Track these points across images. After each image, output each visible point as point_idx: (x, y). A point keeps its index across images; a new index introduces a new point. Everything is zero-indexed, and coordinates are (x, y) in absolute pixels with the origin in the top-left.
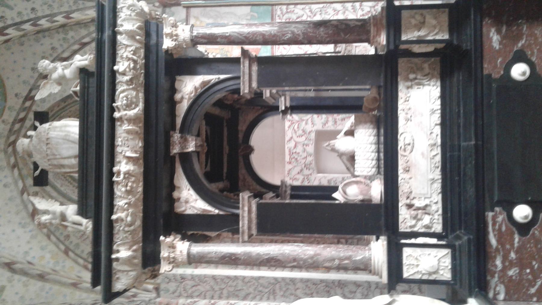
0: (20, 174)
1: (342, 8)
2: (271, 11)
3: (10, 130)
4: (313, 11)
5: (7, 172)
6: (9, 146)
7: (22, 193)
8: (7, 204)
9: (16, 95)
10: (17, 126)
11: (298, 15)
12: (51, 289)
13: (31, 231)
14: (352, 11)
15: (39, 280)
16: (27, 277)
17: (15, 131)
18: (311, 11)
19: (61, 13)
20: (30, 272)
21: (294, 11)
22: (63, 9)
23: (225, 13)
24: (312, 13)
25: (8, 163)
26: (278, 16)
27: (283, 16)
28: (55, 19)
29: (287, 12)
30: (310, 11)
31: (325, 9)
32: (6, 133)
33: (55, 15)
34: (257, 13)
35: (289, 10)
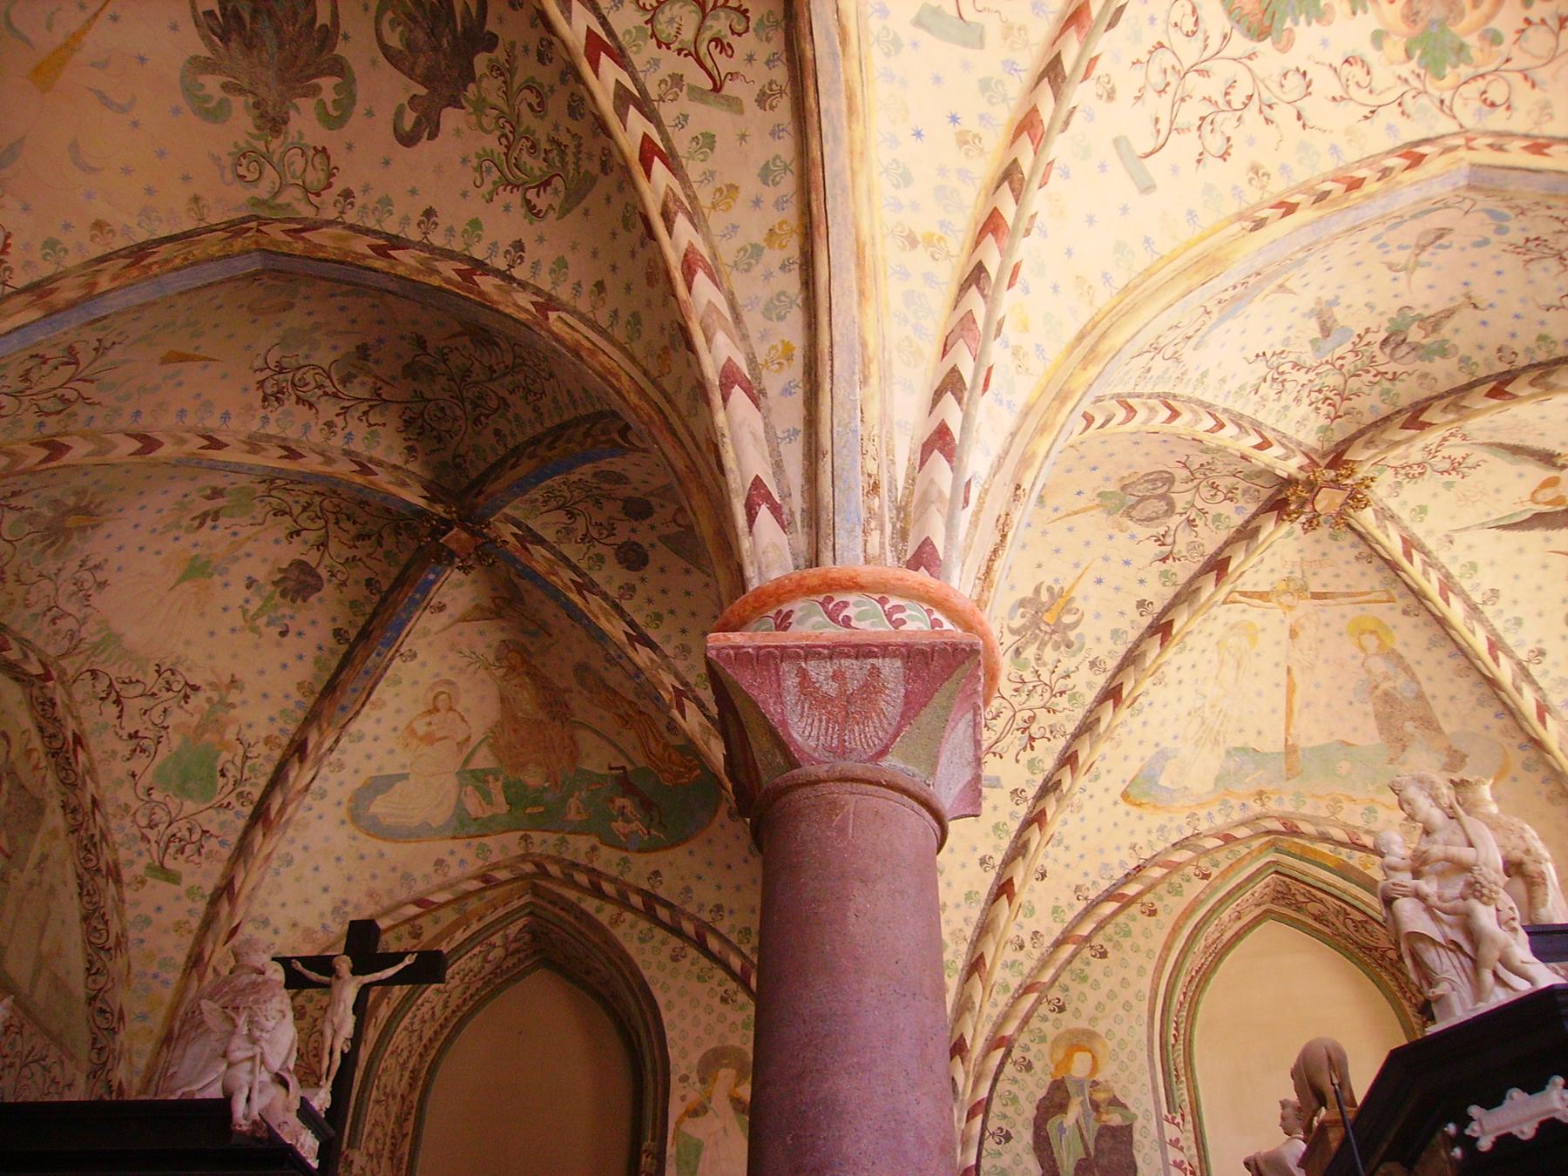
0: (468, 895)
3: (574, 865)
5: (475, 865)
6: (537, 865)
7: (419, 902)
8: (394, 869)
9: (656, 873)
10: (582, 879)
12: (165, 983)
13: (324, 926)
15: (189, 957)
16: (200, 929)
17: (572, 876)
20: (210, 935)
25: (496, 866)
32: (568, 856)
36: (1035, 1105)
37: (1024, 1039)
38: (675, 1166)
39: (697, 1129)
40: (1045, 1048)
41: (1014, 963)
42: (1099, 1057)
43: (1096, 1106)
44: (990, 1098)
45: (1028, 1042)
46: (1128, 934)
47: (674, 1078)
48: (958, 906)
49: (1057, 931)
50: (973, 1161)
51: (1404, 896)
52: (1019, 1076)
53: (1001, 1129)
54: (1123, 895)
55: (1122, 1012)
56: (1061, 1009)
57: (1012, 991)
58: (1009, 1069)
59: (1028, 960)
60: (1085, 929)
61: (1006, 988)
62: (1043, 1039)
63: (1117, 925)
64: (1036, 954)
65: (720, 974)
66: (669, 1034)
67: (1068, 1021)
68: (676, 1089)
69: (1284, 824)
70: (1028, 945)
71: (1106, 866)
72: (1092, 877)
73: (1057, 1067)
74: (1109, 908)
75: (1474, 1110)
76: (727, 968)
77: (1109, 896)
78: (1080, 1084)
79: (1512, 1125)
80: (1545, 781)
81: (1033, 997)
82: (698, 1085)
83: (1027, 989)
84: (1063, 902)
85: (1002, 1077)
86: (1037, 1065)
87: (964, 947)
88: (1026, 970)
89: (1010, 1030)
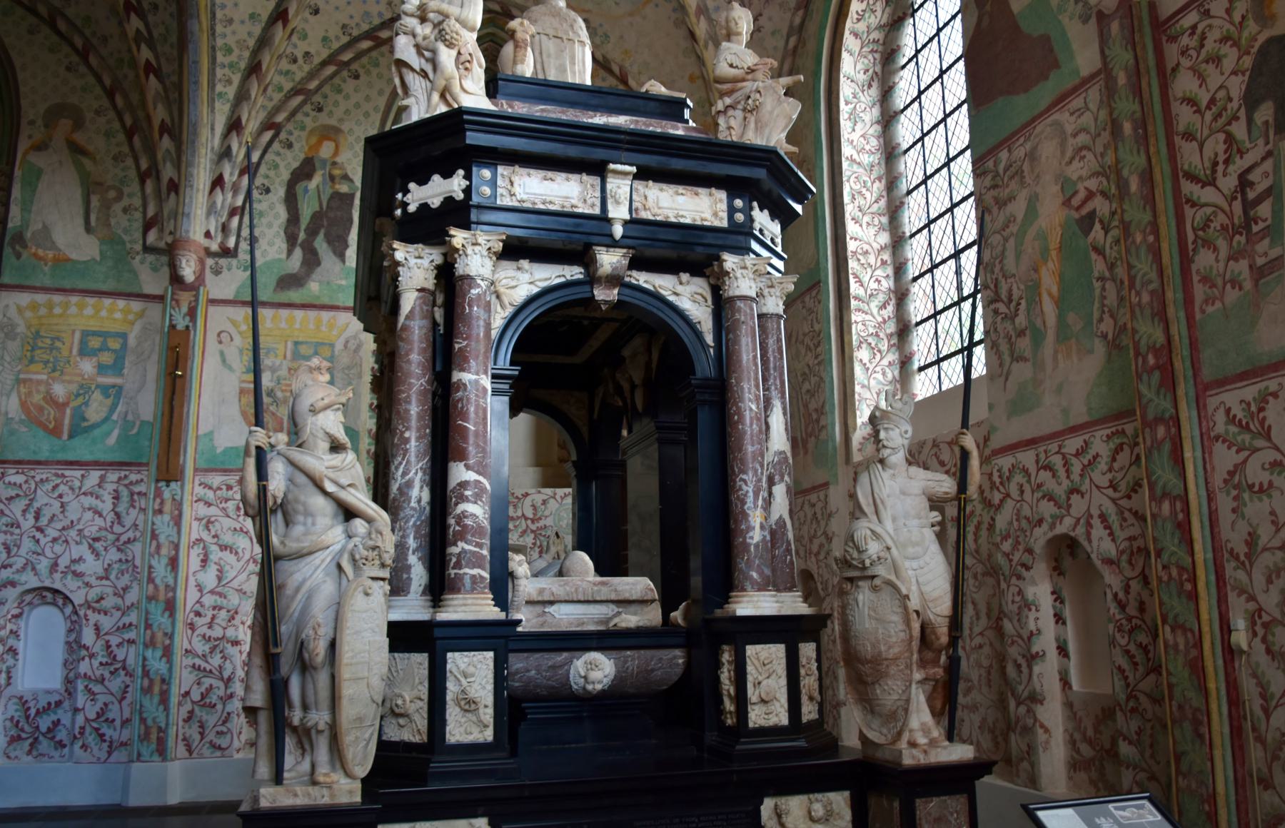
1: (128, 603)
2: (139, 461)
4: (129, 546)
11: (124, 514)
14: (121, 624)
18: (129, 541)
19: (157, 57)
21: (134, 507)
22: (163, 60)
23: (145, 370)
24: (125, 543)
26: (126, 477)
27: (126, 486)
28: (143, 46)
29: (132, 494)
30: (129, 539)
31: (130, 569)
33: (152, 47)
34: (138, 433)
35: (136, 497)
36: (290, 171)
37: (290, 126)
38: (19, 185)
39: (38, 160)
40: (304, 134)
41: (288, 72)
42: (341, 148)
43: (332, 178)
44: (259, 163)
45: (292, 128)
46: (377, 65)
47: (24, 122)
48: (243, 22)
49: (325, 54)
50: (239, 202)
51: (405, 33)
52: (282, 151)
53: (264, 185)
54: (378, 38)
55: (362, 118)
56: (320, 110)
57: (285, 91)
58: (276, 146)
59: (301, 70)
60: (347, 57)
61: (280, 89)
62: (303, 128)
63: (370, 58)
64: (307, 68)
65: (66, 49)
66: (22, 89)
67: (324, 119)
68: (25, 131)
69: (502, 8)
70: (300, 61)
71: (367, 14)
72: (356, 20)
73: (310, 148)
74: (366, 44)
75: (412, 186)
76: (72, 46)
77: (367, 35)
78: (324, 162)
79: (429, 198)
80: (675, 10)
81: (299, 99)
82: (42, 129)
83: (295, 92)
84: (331, 34)
85: (270, 150)
86: (297, 146)
87: (247, 54)
88: (298, 78)
89: (280, 118)
